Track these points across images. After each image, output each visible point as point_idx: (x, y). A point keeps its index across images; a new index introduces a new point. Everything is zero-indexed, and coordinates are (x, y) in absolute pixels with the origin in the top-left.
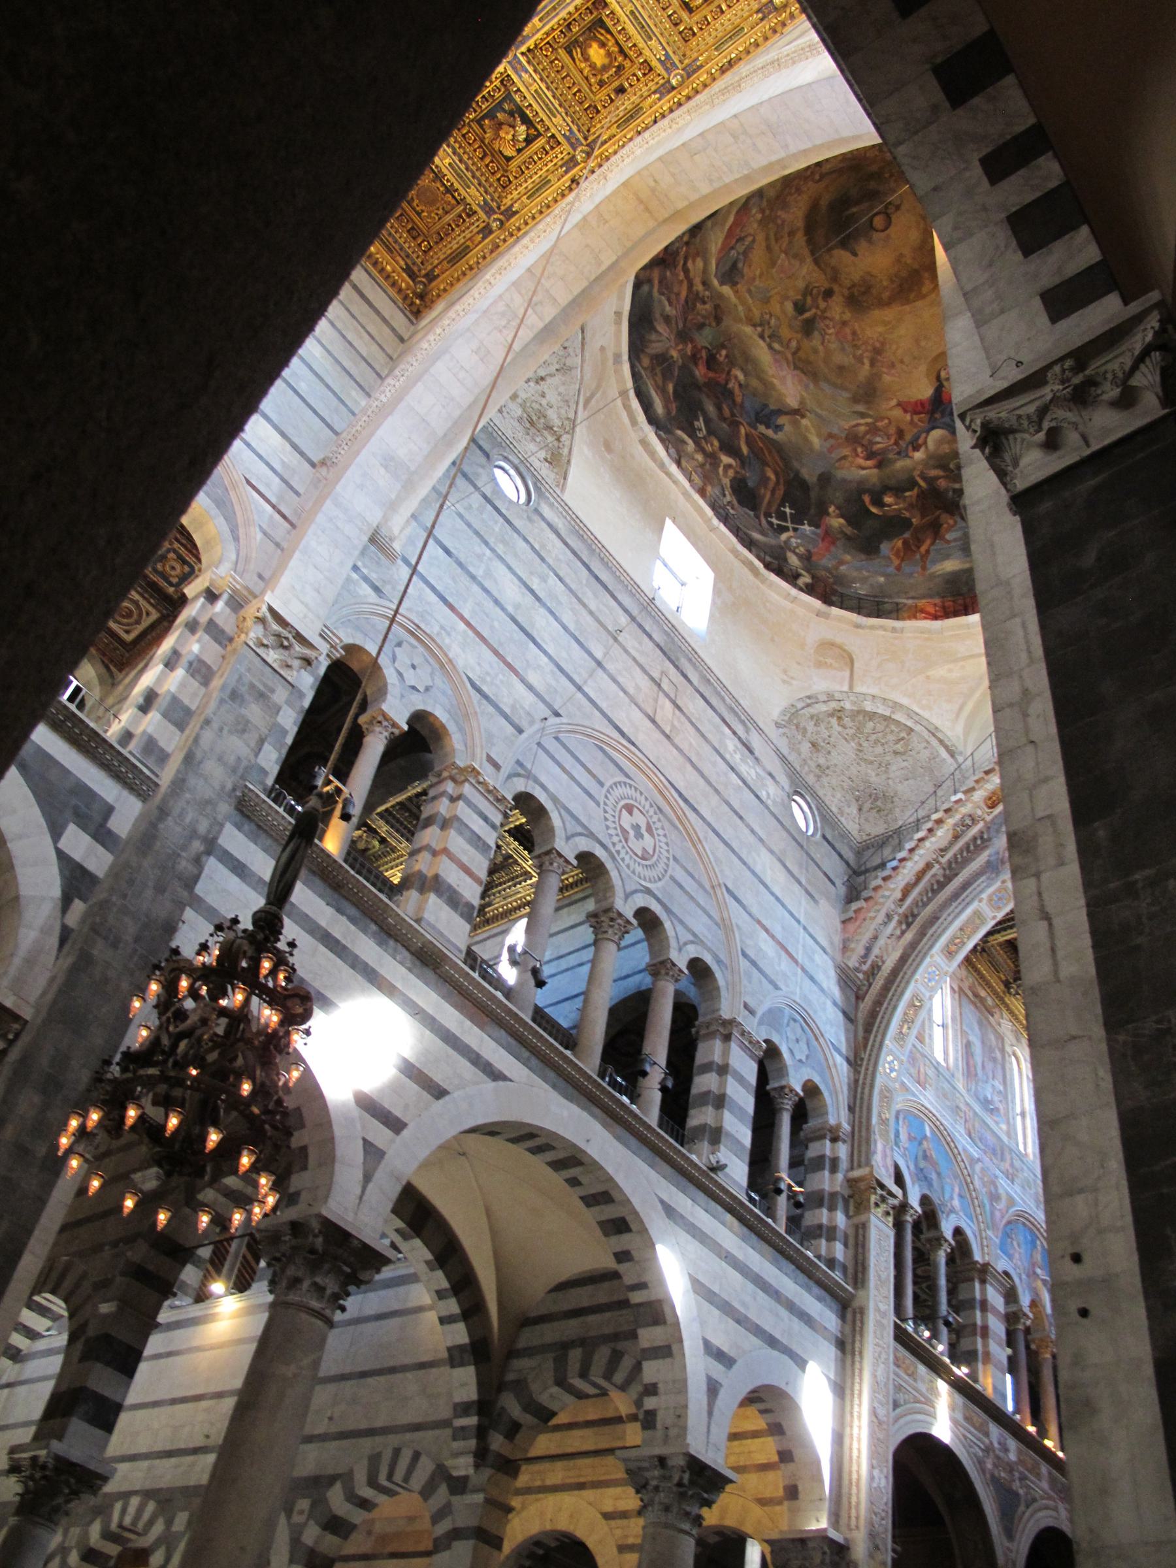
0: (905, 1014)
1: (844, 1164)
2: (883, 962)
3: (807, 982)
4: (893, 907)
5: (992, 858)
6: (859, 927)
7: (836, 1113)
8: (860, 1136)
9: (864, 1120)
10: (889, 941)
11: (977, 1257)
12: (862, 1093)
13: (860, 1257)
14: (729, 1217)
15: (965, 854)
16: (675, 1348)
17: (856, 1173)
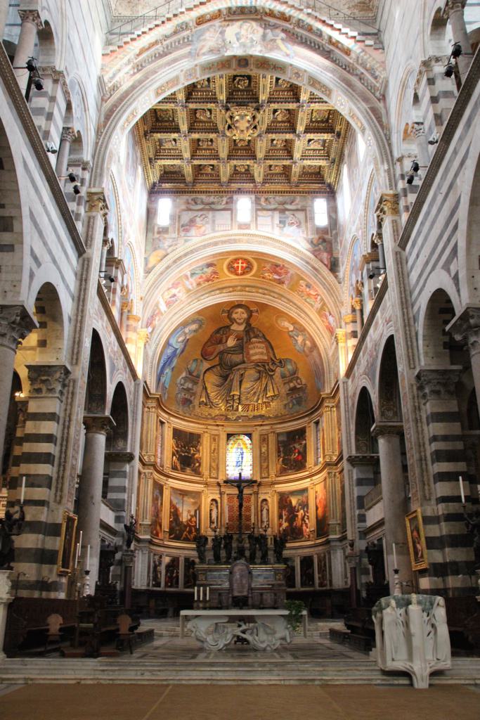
0: (129, 117)
1: (87, 183)
2: (121, 86)
3: (87, 76)
4: (133, 57)
5: (193, 51)
6: (112, 60)
7: (87, 155)
8: (96, 172)
9: (100, 163)
10: (125, 75)
11: (116, 256)
12: (100, 150)
13: (90, 233)
14: (47, 184)
15: (177, 44)
16: (16, 247)
17: (93, 190)
